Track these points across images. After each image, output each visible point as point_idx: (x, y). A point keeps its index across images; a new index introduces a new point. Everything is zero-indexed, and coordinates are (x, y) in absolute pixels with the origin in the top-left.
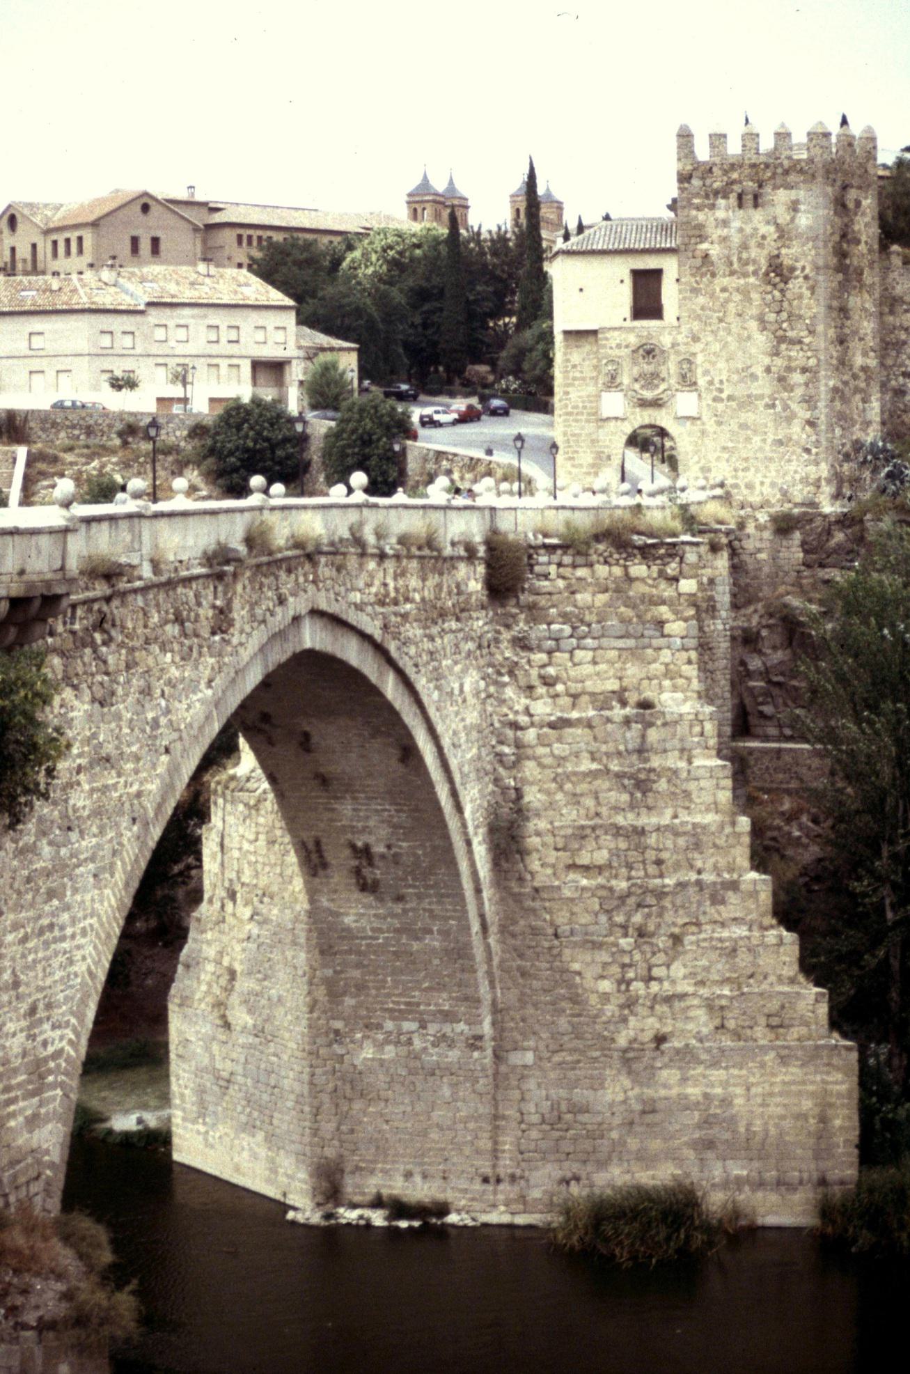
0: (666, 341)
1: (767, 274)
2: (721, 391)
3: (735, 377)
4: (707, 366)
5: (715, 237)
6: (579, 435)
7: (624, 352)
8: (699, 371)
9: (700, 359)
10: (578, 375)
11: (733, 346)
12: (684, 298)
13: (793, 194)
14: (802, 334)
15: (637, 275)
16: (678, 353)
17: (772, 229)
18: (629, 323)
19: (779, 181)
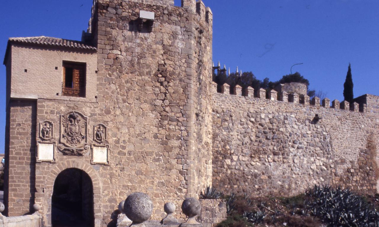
0: (87, 111)
1: (156, 75)
2: (124, 148)
3: (133, 140)
4: (115, 130)
5: (123, 48)
6: (21, 173)
7: (55, 117)
8: (110, 133)
9: (110, 126)
10: (21, 131)
11: (133, 119)
12: (101, 84)
13: (174, 27)
14: (178, 115)
15: (69, 67)
16: (95, 120)
17: (160, 47)
18: (61, 97)
19: (166, 18)
